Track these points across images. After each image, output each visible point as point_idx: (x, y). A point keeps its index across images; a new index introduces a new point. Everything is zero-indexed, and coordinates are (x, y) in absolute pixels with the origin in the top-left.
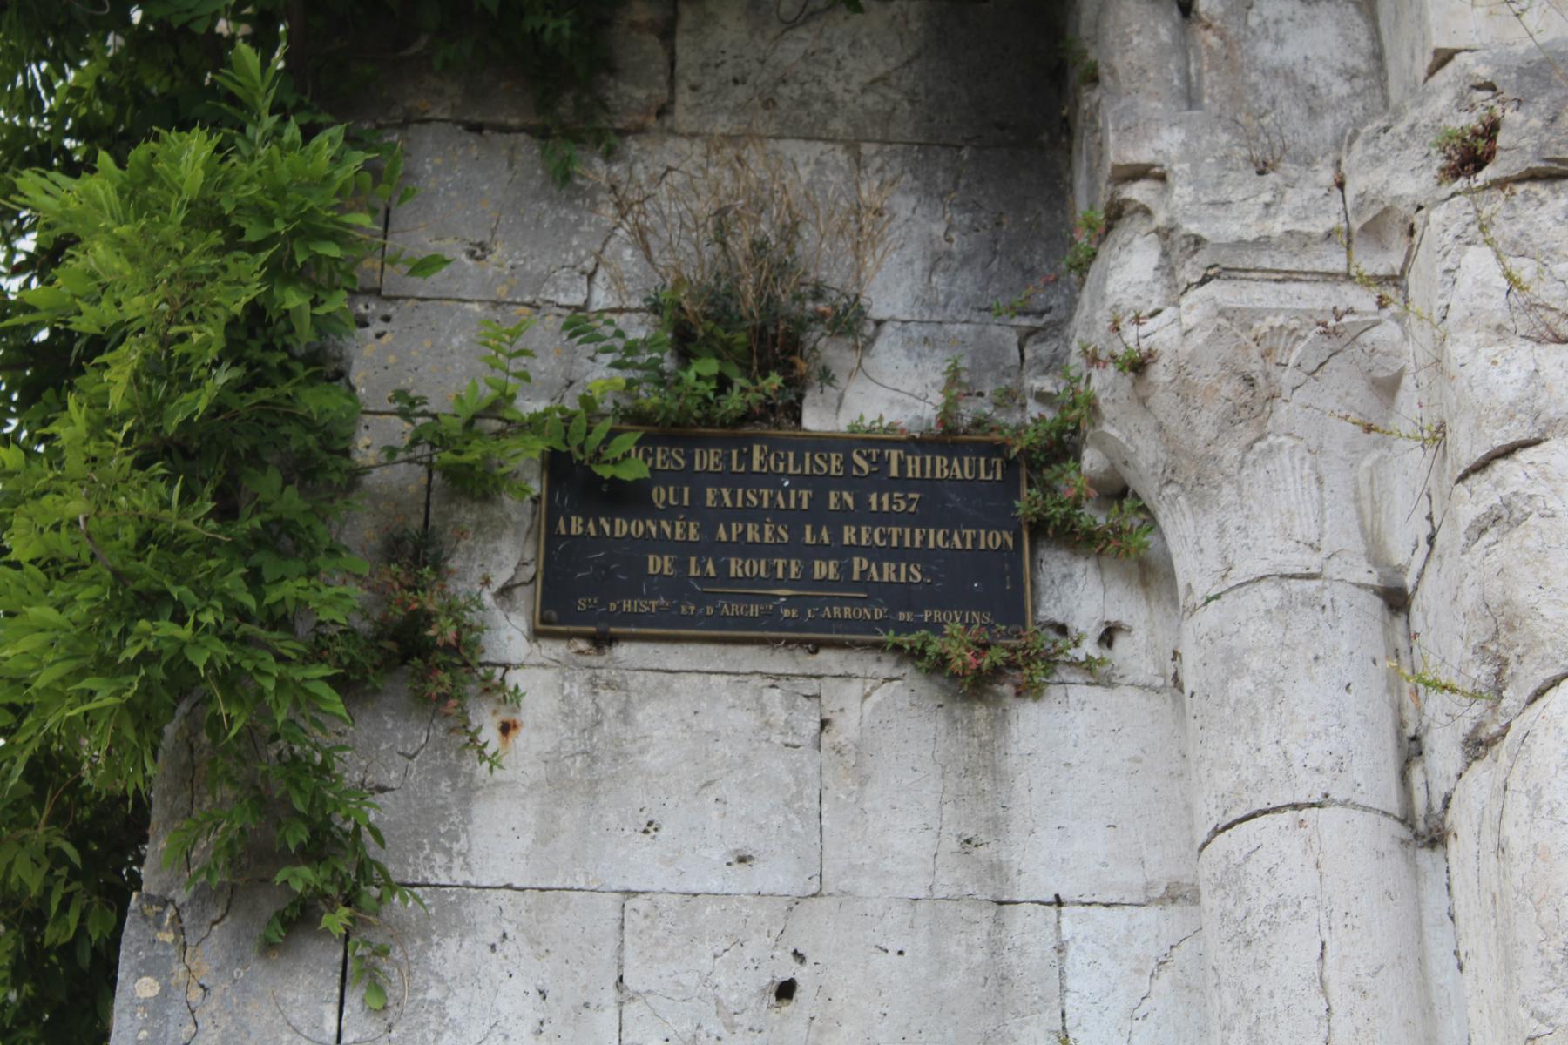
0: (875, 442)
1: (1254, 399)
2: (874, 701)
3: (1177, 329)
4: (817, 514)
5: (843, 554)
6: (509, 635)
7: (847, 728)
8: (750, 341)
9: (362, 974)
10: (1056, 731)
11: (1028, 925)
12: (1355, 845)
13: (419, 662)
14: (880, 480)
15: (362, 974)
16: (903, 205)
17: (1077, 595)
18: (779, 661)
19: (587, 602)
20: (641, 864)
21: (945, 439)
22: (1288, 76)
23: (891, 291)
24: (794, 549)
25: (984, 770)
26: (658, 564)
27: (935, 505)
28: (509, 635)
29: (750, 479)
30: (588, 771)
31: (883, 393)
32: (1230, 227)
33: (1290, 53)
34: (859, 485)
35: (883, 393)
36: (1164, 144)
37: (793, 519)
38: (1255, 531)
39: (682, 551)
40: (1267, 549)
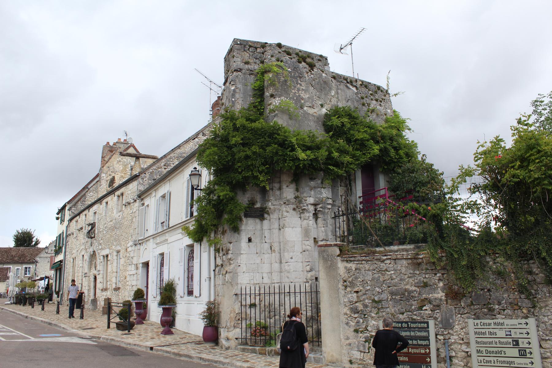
0: (258, 208)
1: (275, 211)
2: (258, 221)
3: (272, 207)
6: (243, 217)
8: (252, 203)
9: (239, 234)
10: (266, 222)
12: (277, 230)
13: (241, 220)
15: (239, 234)
17: (266, 216)
19: (246, 216)
20: (249, 228)
21: (261, 208)
23: (258, 200)
25: (262, 224)
27: (260, 211)
28: (243, 217)
30: (247, 224)
31: (258, 205)
35: (258, 205)
36: (272, 198)
38: (274, 216)
40: (275, 217)
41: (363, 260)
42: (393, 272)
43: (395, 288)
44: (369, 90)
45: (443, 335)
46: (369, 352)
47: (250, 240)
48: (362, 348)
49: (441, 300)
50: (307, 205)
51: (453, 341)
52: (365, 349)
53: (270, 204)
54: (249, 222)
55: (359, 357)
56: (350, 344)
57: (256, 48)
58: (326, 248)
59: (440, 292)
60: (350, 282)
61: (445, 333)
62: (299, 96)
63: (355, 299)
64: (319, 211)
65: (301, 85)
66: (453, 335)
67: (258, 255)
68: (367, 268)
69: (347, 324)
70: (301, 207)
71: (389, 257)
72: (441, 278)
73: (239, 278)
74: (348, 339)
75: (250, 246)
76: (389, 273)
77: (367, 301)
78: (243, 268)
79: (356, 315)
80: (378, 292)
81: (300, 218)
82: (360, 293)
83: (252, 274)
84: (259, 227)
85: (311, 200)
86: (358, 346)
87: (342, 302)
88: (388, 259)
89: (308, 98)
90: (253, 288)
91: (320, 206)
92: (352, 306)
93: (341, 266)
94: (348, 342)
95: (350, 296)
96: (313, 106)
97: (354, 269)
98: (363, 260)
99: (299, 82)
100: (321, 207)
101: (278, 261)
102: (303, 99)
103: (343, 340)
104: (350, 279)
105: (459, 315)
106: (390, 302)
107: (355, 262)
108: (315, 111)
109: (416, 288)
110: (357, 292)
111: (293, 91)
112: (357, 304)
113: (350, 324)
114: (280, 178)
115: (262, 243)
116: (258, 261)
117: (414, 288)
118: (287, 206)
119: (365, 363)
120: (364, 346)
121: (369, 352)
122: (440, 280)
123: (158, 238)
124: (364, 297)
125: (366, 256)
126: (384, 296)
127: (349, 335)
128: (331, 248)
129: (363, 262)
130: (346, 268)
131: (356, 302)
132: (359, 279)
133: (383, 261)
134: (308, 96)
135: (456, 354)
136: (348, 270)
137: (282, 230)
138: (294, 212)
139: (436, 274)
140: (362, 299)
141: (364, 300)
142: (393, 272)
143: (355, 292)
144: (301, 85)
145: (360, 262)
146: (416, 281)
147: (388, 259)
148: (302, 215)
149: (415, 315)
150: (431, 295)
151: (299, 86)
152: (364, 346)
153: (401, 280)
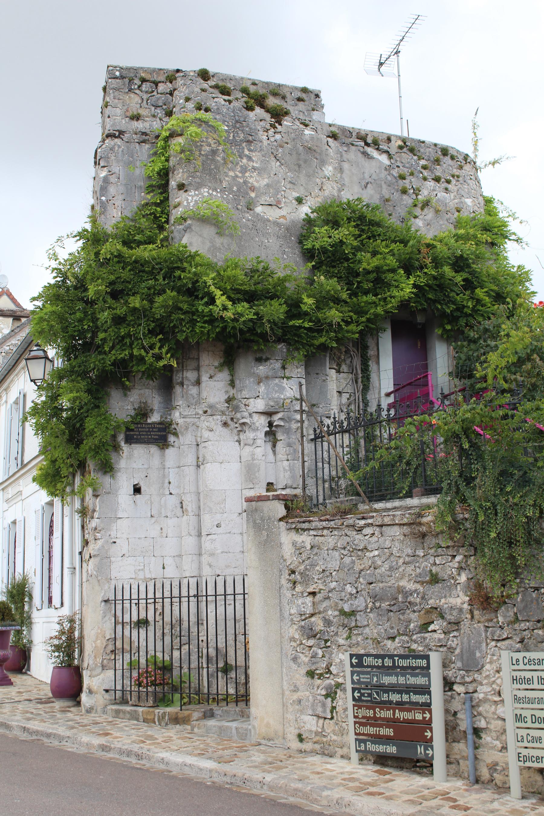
0: (154, 423)
1: (187, 428)
2: (154, 449)
3: (181, 421)
4: (149, 431)
5: (151, 435)
6: (122, 444)
7: (152, 452)
8: (143, 412)
9: (113, 476)
10: (170, 452)
11: (166, 470)
12: (193, 469)
13: (116, 448)
14: (154, 428)
15: (113, 476)
16: (157, 396)
17: (171, 439)
18: (146, 446)
19: (129, 440)
20: (135, 466)
21: (160, 423)
22: (191, 395)
23: (156, 407)
24: (147, 435)
25: (163, 456)
26: (135, 437)
27: (160, 430)
28: (122, 444)
29: (143, 428)
30: (130, 457)
31: (155, 418)
32: (186, 413)
33: (192, 392)
34: (153, 428)
35: (155, 418)
36: (180, 403)
37: (147, 432)
38: (186, 439)
39: (137, 435)
40: (187, 442)
41: (324, 528)
42: (376, 553)
43: (381, 585)
44: (420, 158)
45: (463, 684)
46: (332, 718)
47: (137, 490)
48: (319, 711)
49: (461, 610)
50: (250, 415)
51: (481, 696)
52: (324, 711)
53: (177, 414)
54: (135, 452)
55: (314, 729)
56: (300, 701)
57: (156, 84)
58: (260, 503)
59: (461, 594)
60: (301, 574)
61: (468, 679)
62: (245, 182)
63: (309, 610)
64: (277, 426)
65: (250, 158)
66: (481, 684)
67: (153, 520)
68: (331, 546)
69: (295, 659)
70: (238, 419)
71: (370, 521)
72: (463, 565)
73: (112, 567)
74: (296, 689)
75: (138, 502)
76: (372, 555)
77: (330, 612)
78: (122, 546)
79: (311, 642)
80: (351, 594)
81: (239, 441)
82: (319, 597)
83: (140, 559)
84: (156, 462)
85: (260, 405)
86: (313, 705)
87: (286, 615)
88: (368, 525)
89: (268, 185)
90: (143, 589)
91: (280, 415)
92: (303, 623)
93: (287, 540)
94: (295, 697)
95: (300, 601)
96: (279, 202)
97: (309, 547)
98: (324, 528)
99: (247, 152)
100: (281, 419)
101: (194, 532)
102: (253, 189)
103: (287, 693)
104: (302, 567)
105: (493, 643)
106: (371, 615)
107: (312, 532)
108: (283, 212)
109: (418, 586)
110: (313, 594)
111: (231, 174)
112: (313, 619)
113: (299, 661)
114: (198, 359)
115: (164, 495)
116: (154, 532)
117: (411, 586)
118: (211, 419)
119: (325, 739)
120: (324, 705)
121: (332, 718)
122: (460, 569)
123: (10, 489)
124: (324, 604)
125: (328, 520)
126: (360, 603)
127: (298, 684)
128: (268, 502)
129: (325, 532)
130: (294, 544)
131: (312, 615)
132: (318, 568)
133: (360, 530)
134: (266, 181)
135: (488, 723)
136: (299, 549)
137: (202, 467)
138: (225, 431)
139: (454, 556)
140: (321, 608)
141: (325, 611)
142: (376, 553)
143: (310, 593)
144: (250, 158)
145: (320, 533)
146: (418, 570)
147: (368, 525)
148: (242, 436)
149: (415, 642)
150: (443, 601)
151: (245, 161)
152: (324, 705)
153: (391, 569)
